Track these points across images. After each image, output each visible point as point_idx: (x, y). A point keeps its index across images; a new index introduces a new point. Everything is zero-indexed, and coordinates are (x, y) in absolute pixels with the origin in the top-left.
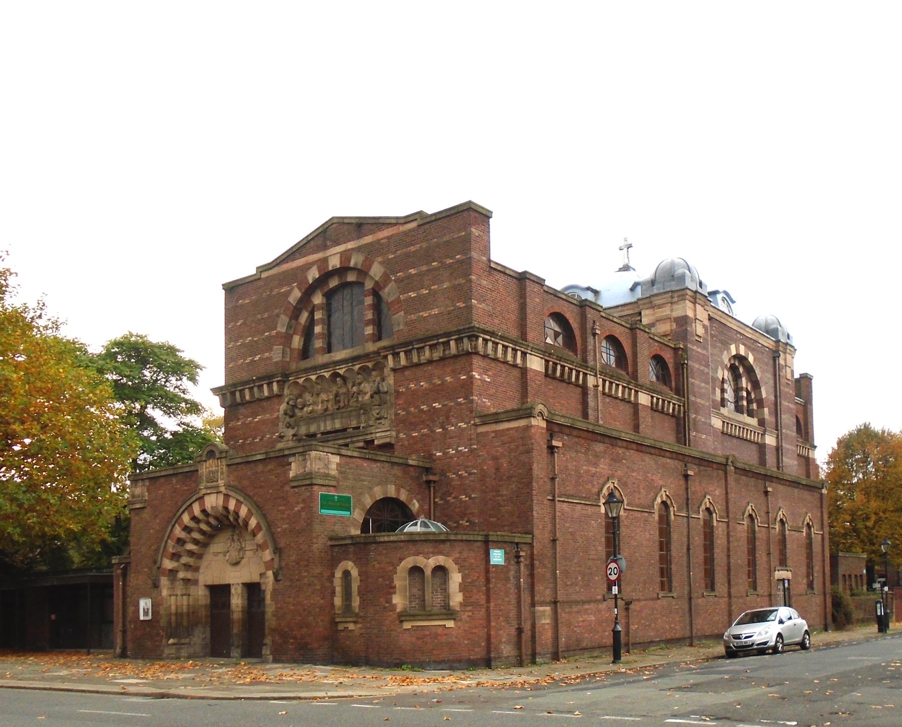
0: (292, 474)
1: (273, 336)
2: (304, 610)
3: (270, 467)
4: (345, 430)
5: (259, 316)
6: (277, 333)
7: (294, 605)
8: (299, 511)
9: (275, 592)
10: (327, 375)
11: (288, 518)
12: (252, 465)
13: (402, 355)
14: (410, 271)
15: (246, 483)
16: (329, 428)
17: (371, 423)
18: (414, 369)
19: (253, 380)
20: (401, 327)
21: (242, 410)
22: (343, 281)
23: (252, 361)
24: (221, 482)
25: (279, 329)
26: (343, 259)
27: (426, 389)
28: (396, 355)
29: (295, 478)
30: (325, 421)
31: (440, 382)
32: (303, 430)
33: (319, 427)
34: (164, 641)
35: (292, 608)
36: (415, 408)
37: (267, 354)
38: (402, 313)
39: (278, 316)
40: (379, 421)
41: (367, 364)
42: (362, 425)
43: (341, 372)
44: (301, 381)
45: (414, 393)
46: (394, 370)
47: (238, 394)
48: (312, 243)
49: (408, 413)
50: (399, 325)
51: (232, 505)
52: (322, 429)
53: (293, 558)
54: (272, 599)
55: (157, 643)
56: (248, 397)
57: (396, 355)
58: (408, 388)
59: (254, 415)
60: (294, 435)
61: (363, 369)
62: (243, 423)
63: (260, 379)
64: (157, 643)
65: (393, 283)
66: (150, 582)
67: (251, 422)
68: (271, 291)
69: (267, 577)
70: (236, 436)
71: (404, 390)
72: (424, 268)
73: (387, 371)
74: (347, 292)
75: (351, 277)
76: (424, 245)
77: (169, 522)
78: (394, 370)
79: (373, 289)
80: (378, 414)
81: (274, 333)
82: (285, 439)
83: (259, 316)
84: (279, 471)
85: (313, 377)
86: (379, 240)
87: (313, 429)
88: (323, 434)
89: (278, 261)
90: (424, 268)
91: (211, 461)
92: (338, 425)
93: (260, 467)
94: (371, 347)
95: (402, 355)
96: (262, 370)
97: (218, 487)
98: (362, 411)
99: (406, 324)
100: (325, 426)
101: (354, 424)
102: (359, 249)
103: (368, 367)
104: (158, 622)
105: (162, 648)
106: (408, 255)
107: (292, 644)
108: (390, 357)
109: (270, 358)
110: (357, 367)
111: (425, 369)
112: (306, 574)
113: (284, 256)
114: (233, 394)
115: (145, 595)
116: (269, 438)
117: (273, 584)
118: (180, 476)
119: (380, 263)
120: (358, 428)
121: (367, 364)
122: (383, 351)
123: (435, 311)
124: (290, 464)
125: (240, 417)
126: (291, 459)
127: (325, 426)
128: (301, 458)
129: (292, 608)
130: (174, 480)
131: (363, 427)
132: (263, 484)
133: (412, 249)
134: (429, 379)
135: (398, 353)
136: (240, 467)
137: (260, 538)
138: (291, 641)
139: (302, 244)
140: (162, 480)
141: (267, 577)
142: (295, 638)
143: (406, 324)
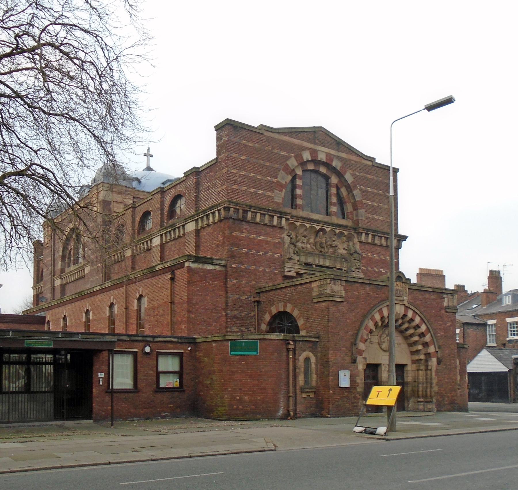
0: (445, 304)
1: (274, 182)
2: (453, 382)
3: (433, 297)
4: (332, 268)
5: (262, 162)
6: (277, 181)
7: (448, 379)
8: (449, 326)
9: (437, 371)
10: (318, 228)
11: (443, 329)
12: (423, 293)
13: (370, 236)
14: (368, 188)
15: (419, 302)
16: (321, 263)
17: (353, 269)
18: (370, 246)
19: (269, 210)
20: (363, 219)
21: (245, 226)
22: (317, 169)
23: (255, 193)
24: (406, 299)
25: (279, 179)
26: (328, 158)
27: (377, 260)
28: (367, 234)
29: (446, 308)
30: (319, 258)
31: (384, 258)
32: (303, 259)
33: (314, 260)
34: (360, 401)
35: (447, 380)
36: (371, 269)
37: (269, 193)
38: (364, 210)
39: (278, 169)
40: (358, 270)
41: (344, 232)
42: (344, 269)
43: (328, 230)
44: (298, 224)
45: (371, 259)
46: (361, 242)
47: (250, 214)
48: (305, 134)
49: (368, 270)
50: (362, 217)
51: (410, 314)
52: (317, 263)
53: (447, 352)
54: (435, 376)
55: (355, 404)
56: (258, 220)
57: (367, 234)
58: (367, 256)
59: (259, 234)
60: (298, 261)
61: (341, 234)
62: (247, 237)
63: (274, 211)
64: (355, 404)
65: (358, 190)
66: (348, 359)
67: (254, 238)
68: (273, 148)
69: (432, 362)
70: (239, 244)
71: (365, 255)
72: (375, 191)
73: (356, 240)
74: (314, 176)
75: (323, 170)
76: (375, 178)
77: (364, 317)
78: (361, 242)
79: (336, 184)
80: (359, 266)
81: (275, 180)
82: (292, 261)
83: (262, 162)
84: (438, 301)
85: (308, 226)
86: (350, 160)
87: (310, 260)
88: (317, 266)
89: (281, 131)
90: (375, 191)
91: (398, 282)
92: (328, 263)
93: (427, 295)
94: (336, 220)
95: (370, 236)
96: (263, 203)
97: (403, 300)
98: (343, 260)
99: (366, 218)
100: (319, 261)
101: (338, 266)
102: (339, 158)
103: (344, 233)
104: (355, 388)
105: (359, 408)
106: (367, 179)
107: (447, 401)
108: (364, 234)
109: (273, 198)
110: (337, 231)
111: (376, 248)
112: (453, 362)
113: (286, 131)
114: (245, 212)
115: (345, 368)
116: (271, 255)
117: (436, 366)
118: (372, 286)
119: (351, 174)
120: (341, 269)
121: (344, 232)
122: (362, 229)
123: (381, 218)
124: (444, 298)
125: (244, 231)
126: (445, 296)
127: (319, 261)
128: (451, 297)
129: (447, 380)
130: (368, 288)
131: (345, 270)
132: (429, 306)
133: (369, 176)
134: (379, 254)
135: (369, 234)
136: (415, 292)
137: (428, 338)
138: (446, 399)
139: (299, 130)
140: (357, 285)
141: (432, 362)
142: (448, 397)
143: (366, 218)
